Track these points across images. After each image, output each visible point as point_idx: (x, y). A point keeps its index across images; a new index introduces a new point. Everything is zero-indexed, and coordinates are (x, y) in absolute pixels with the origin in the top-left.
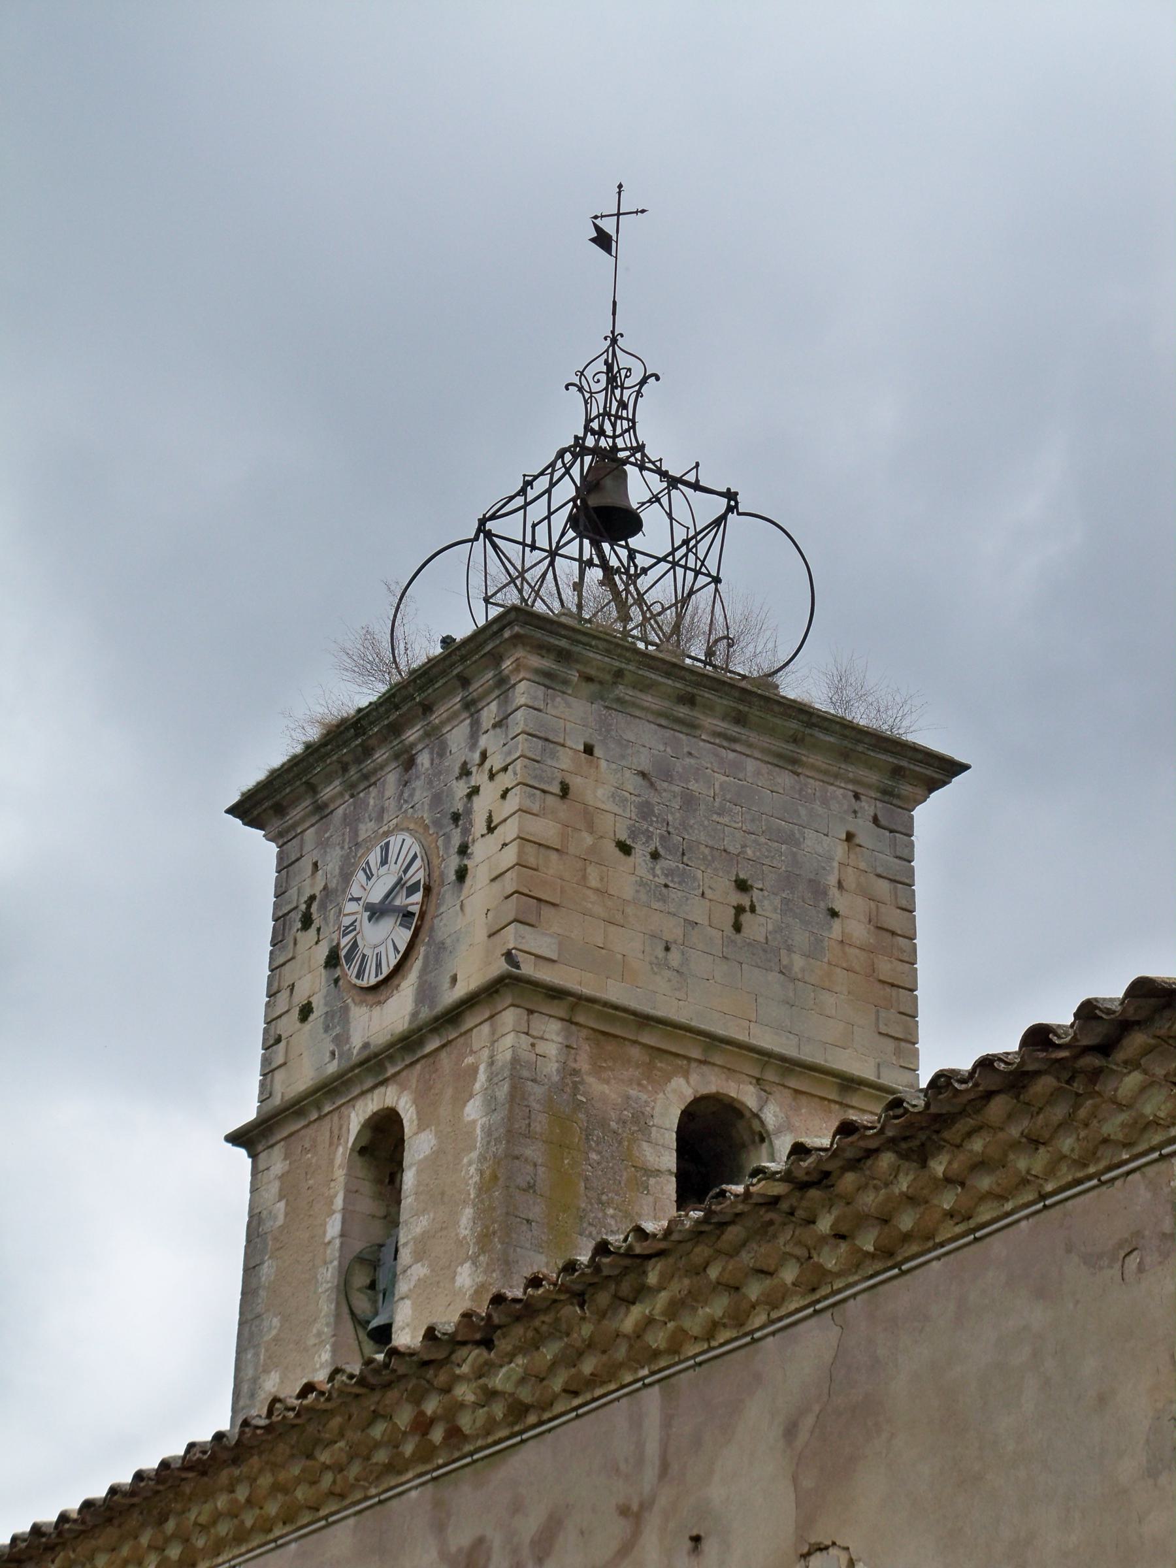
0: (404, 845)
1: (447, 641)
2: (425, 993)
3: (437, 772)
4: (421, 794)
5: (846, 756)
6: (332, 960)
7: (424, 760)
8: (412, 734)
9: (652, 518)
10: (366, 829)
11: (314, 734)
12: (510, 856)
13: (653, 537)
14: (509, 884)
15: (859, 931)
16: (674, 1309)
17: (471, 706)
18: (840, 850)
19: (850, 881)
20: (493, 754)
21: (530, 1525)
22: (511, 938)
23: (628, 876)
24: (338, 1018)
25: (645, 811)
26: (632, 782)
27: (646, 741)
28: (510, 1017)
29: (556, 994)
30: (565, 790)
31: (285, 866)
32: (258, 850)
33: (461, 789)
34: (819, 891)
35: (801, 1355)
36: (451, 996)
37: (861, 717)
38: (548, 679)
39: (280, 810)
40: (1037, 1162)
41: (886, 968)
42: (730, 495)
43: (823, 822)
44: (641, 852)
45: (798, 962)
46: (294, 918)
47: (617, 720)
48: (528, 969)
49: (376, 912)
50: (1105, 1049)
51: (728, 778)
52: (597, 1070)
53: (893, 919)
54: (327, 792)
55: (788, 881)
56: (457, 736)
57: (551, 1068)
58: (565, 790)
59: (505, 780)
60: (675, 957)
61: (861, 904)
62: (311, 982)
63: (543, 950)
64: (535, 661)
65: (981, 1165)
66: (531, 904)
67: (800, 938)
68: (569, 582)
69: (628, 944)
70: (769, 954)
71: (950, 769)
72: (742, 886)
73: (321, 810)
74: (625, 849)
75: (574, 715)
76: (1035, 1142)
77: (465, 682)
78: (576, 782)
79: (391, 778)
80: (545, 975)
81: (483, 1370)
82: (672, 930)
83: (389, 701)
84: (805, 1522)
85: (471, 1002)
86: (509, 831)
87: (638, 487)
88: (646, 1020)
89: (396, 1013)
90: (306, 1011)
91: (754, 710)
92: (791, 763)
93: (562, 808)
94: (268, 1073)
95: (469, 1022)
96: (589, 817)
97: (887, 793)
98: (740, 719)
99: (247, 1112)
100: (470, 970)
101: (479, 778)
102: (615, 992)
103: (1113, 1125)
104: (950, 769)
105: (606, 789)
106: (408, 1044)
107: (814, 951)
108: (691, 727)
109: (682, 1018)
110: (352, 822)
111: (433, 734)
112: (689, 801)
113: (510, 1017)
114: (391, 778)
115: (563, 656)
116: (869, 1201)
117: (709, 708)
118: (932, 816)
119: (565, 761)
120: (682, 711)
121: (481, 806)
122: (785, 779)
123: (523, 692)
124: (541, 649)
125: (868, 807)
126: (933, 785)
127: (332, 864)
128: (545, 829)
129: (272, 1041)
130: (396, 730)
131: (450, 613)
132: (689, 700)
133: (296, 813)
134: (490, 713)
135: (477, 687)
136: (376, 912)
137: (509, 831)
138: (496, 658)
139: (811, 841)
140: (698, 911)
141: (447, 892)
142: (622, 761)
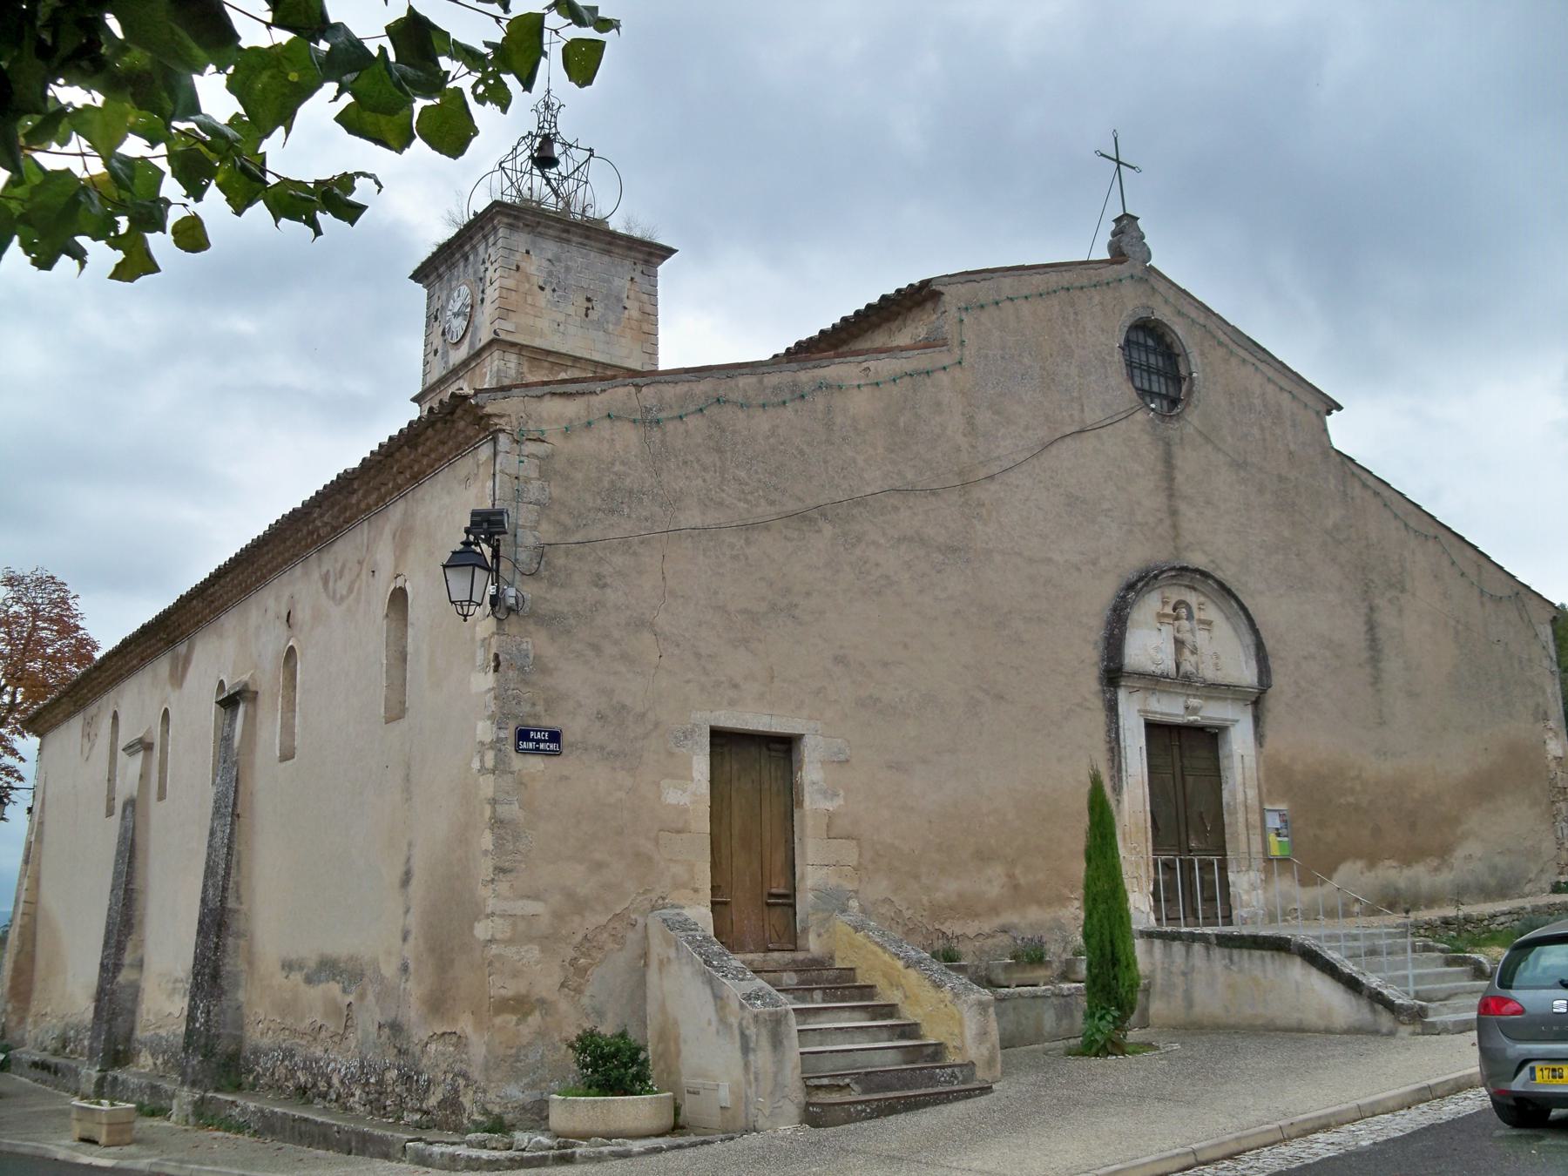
0: (464, 289)
1: (475, 214)
2: (472, 345)
3: (476, 261)
4: (470, 271)
5: (630, 249)
6: (443, 333)
7: (471, 258)
8: (467, 248)
9: (562, 159)
10: (454, 283)
11: (435, 249)
12: (497, 294)
13: (563, 167)
14: (496, 304)
15: (635, 313)
16: (365, 497)
17: (485, 237)
18: (628, 284)
19: (632, 294)
20: (492, 253)
21: (338, 566)
22: (496, 325)
23: (543, 299)
24: (446, 354)
25: (550, 274)
26: (545, 264)
27: (551, 248)
28: (496, 354)
29: (513, 345)
30: (518, 268)
31: (430, 297)
32: (420, 291)
33: (482, 268)
34: (619, 300)
35: (397, 511)
36: (479, 346)
37: (637, 234)
38: (511, 226)
39: (427, 277)
40: (445, 449)
41: (646, 327)
42: (591, 150)
43: (621, 276)
44: (548, 290)
45: (611, 327)
46: (433, 317)
47: (539, 240)
48: (503, 336)
49: (456, 315)
50: (452, 413)
51: (584, 262)
52: (531, 372)
53: (648, 309)
54: (441, 270)
55: (607, 297)
56: (481, 249)
57: (513, 372)
58: (518, 268)
59: (496, 265)
60: (562, 328)
61: (637, 304)
62: (437, 341)
63: (509, 329)
64: (506, 220)
65: (431, 450)
66: (505, 312)
67: (612, 318)
68: (536, 185)
69: (543, 324)
70: (600, 325)
71: (671, 251)
72: (589, 300)
73: (440, 277)
74: (542, 289)
75: (521, 240)
76: (443, 443)
77: (482, 228)
78: (522, 265)
79: (462, 264)
80: (509, 338)
81: (321, 516)
82: (561, 318)
83: (458, 235)
84: (396, 567)
85: (483, 349)
86: (496, 285)
87: (557, 149)
88: (549, 353)
89: (462, 353)
90: (436, 352)
91: (595, 234)
92: (609, 252)
93: (517, 275)
94: (425, 375)
95: (485, 355)
96: (528, 277)
97: (646, 262)
98: (587, 237)
99: (418, 389)
100: (485, 336)
101: (488, 264)
102: (537, 343)
103: (461, 438)
104: (671, 251)
105: (535, 267)
106: (465, 364)
107: (618, 322)
108: (568, 241)
109: (563, 351)
110: (449, 281)
111: (474, 248)
112: (568, 269)
113: (496, 354)
114: (462, 264)
115: (516, 218)
116: (405, 461)
117: (575, 234)
118: (663, 269)
119: (518, 257)
120: (564, 235)
121: (489, 274)
122: (606, 258)
123: (501, 232)
124: (508, 215)
125: (639, 267)
126: (665, 258)
127: (444, 297)
128: (510, 283)
129: (426, 363)
130: (461, 246)
131: (481, 203)
132: (568, 231)
133: (432, 278)
134: (491, 240)
135: (487, 230)
136: (456, 315)
137: (496, 285)
138: (492, 219)
139: (617, 282)
140: (571, 310)
141: (477, 307)
142: (538, 257)
